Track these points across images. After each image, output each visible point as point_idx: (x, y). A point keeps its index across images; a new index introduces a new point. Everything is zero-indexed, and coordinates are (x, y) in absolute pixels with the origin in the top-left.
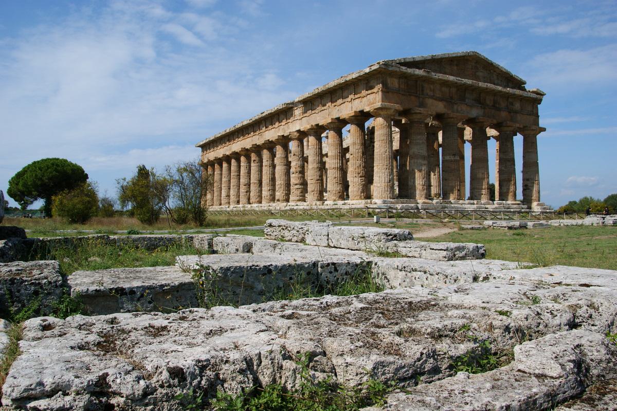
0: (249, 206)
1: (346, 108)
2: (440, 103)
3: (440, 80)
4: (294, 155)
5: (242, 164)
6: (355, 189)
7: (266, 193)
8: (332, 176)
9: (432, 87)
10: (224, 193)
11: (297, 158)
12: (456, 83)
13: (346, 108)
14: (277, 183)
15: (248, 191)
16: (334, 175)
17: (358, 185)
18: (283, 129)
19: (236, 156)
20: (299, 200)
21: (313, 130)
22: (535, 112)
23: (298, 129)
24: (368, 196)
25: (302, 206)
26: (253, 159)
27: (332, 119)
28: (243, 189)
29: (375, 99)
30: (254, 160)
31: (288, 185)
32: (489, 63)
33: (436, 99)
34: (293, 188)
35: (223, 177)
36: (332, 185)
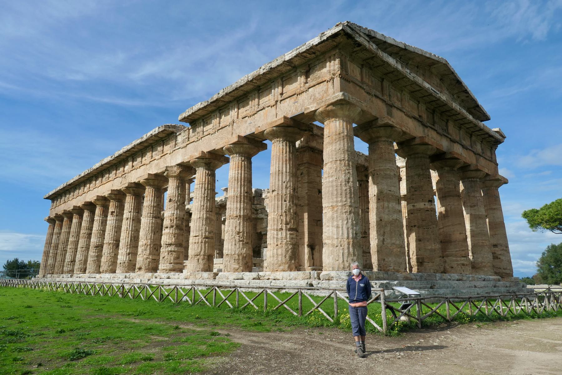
0: (98, 276)
3: (415, 83)
4: (170, 200)
5: (96, 218)
6: (280, 251)
7: (122, 256)
8: (231, 229)
9: (399, 94)
10: (68, 258)
11: (173, 205)
12: (431, 95)
15: (99, 257)
16: (237, 229)
17: (286, 244)
18: (157, 165)
19: (90, 206)
20: (171, 270)
23: (179, 161)
26: (111, 209)
27: (239, 136)
28: (92, 253)
29: (326, 91)
31: (156, 247)
33: (407, 115)
34: (164, 251)
35: (71, 236)
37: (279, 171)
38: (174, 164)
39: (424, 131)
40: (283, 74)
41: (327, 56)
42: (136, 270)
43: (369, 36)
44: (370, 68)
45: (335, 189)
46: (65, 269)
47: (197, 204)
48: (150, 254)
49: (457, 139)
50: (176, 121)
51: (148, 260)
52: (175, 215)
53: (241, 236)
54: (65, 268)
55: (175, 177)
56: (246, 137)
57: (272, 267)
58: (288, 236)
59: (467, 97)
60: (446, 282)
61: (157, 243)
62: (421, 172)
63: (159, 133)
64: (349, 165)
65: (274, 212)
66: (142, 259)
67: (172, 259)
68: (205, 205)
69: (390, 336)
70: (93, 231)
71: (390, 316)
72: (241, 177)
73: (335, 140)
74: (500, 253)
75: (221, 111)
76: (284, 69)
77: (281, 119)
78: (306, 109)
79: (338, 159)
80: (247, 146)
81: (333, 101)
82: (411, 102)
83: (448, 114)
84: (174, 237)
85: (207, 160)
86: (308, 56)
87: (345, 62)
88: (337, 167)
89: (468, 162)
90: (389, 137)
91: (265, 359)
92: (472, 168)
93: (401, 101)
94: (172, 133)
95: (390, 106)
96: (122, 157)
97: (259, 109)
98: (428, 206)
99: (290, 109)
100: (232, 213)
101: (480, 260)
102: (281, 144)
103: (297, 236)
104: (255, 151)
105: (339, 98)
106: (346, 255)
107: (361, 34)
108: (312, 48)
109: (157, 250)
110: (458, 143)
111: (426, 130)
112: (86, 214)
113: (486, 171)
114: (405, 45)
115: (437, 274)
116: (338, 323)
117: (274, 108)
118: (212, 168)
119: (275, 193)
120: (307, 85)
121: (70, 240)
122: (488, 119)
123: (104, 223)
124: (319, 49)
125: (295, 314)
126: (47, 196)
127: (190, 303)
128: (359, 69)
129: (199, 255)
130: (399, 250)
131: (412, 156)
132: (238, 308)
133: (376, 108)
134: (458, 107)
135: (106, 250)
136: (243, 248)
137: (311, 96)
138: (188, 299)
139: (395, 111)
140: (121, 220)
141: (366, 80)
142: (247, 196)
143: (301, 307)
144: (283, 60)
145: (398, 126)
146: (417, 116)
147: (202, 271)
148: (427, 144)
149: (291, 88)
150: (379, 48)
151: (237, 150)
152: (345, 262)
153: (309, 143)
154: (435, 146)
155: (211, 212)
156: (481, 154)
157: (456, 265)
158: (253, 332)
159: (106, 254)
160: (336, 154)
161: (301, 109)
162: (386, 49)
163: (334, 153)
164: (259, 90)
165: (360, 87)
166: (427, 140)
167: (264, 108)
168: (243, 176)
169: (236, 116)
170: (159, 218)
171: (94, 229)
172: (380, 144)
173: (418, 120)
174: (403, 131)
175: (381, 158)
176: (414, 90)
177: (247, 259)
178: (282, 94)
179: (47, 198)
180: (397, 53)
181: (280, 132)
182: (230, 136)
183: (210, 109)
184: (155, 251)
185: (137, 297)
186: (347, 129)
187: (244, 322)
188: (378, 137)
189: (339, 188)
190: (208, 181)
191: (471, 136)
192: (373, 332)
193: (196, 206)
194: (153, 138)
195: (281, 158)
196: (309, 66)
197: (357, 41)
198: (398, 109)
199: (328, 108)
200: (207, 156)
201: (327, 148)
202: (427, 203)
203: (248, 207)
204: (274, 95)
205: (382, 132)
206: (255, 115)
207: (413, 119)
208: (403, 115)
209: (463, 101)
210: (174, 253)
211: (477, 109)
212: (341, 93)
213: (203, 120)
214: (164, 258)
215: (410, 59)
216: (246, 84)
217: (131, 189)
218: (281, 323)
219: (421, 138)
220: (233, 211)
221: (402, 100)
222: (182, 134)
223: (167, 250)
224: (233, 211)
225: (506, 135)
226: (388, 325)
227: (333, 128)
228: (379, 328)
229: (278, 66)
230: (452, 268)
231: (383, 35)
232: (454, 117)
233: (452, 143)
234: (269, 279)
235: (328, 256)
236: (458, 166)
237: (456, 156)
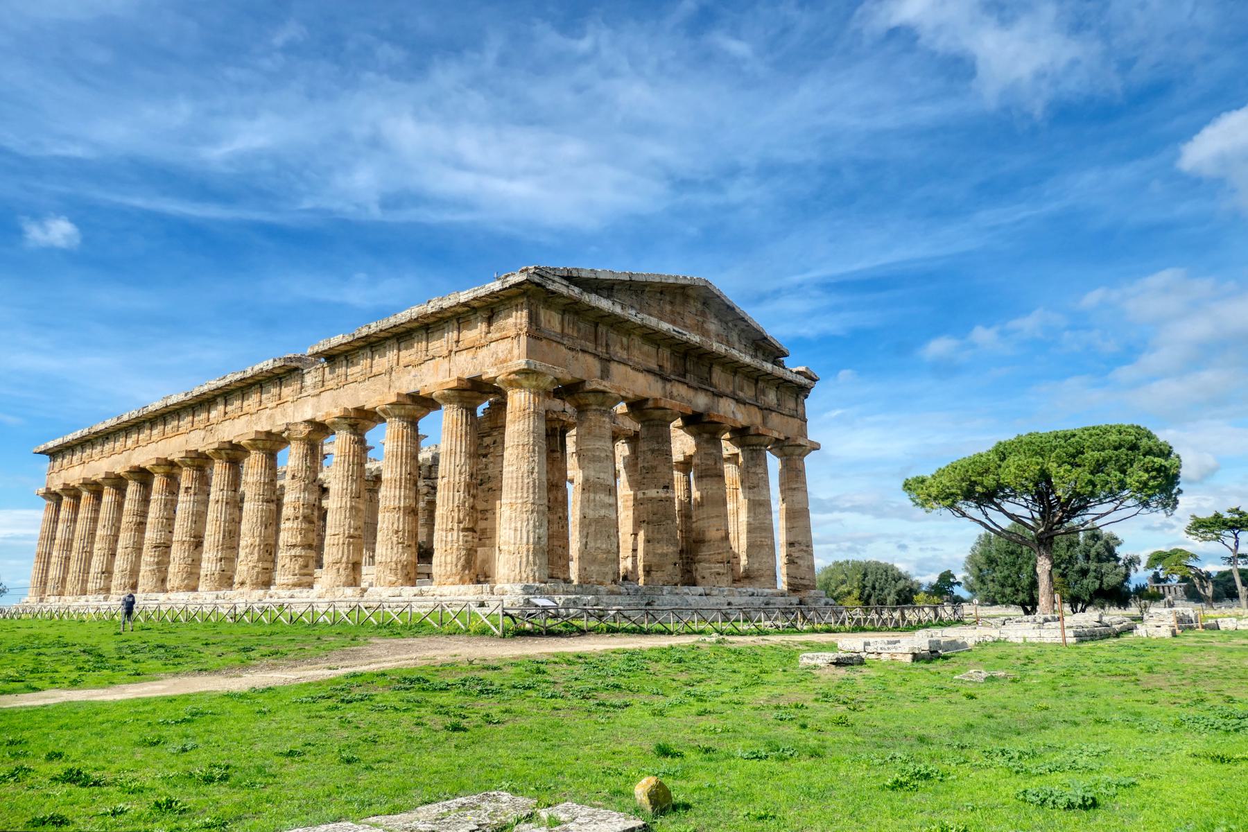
0: (162, 597)
1: (435, 368)
2: (640, 375)
3: (643, 326)
4: (294, 477)
5: (154, 496)
7: (209, 562)
9: (625, 340)
11: (298, 483)
12: (673, 337)
13: (435, 368)
14: (242, 543)
17: (458, 549)
18: (271, 417)
21: (348, 421)
22: (800, 411)
23: (308, 417)
27: (399, 395)
28: (148, 557)
29: (511, 351)
30: (187, 488)
31: (269, 550)
32: (728, 307)
34: (283, 556)
35: (100, 526)
36: (388, 548)
39: (664, 388)
46: (90, 586)
48: (258, 561)
49: (728, 391)
54: (89, 585)
55: (300, 440)
56: (408, 395)
62: (656, 446)
64: (534, 451)
82: (646, 348)
92: (752, 431)
93: (627, 348)
94: (296, 369)
95: (606, 361)
99: (466, 366)
101: (756, 566)
111: (668, 386)
113: (776, 435)
119: (445, 480)
121: (98, 533)
123: (170, 506)
126: (42, 448)
133: (584, 367)
135: (177, 552)
136: (403, 553)
140: (206, 503)
141: (568, 331)
166: (662, 404)
167: (434, 358)
178: (458, 342)
182: (386, 390)
183: (357, 344)
184: (267, 555)
185: (257, 622)
191: (757, 381)
193: (334, 474)
198: (619, 362)
208: (629, 369)
219: (656, 400)
227: (518, 400)
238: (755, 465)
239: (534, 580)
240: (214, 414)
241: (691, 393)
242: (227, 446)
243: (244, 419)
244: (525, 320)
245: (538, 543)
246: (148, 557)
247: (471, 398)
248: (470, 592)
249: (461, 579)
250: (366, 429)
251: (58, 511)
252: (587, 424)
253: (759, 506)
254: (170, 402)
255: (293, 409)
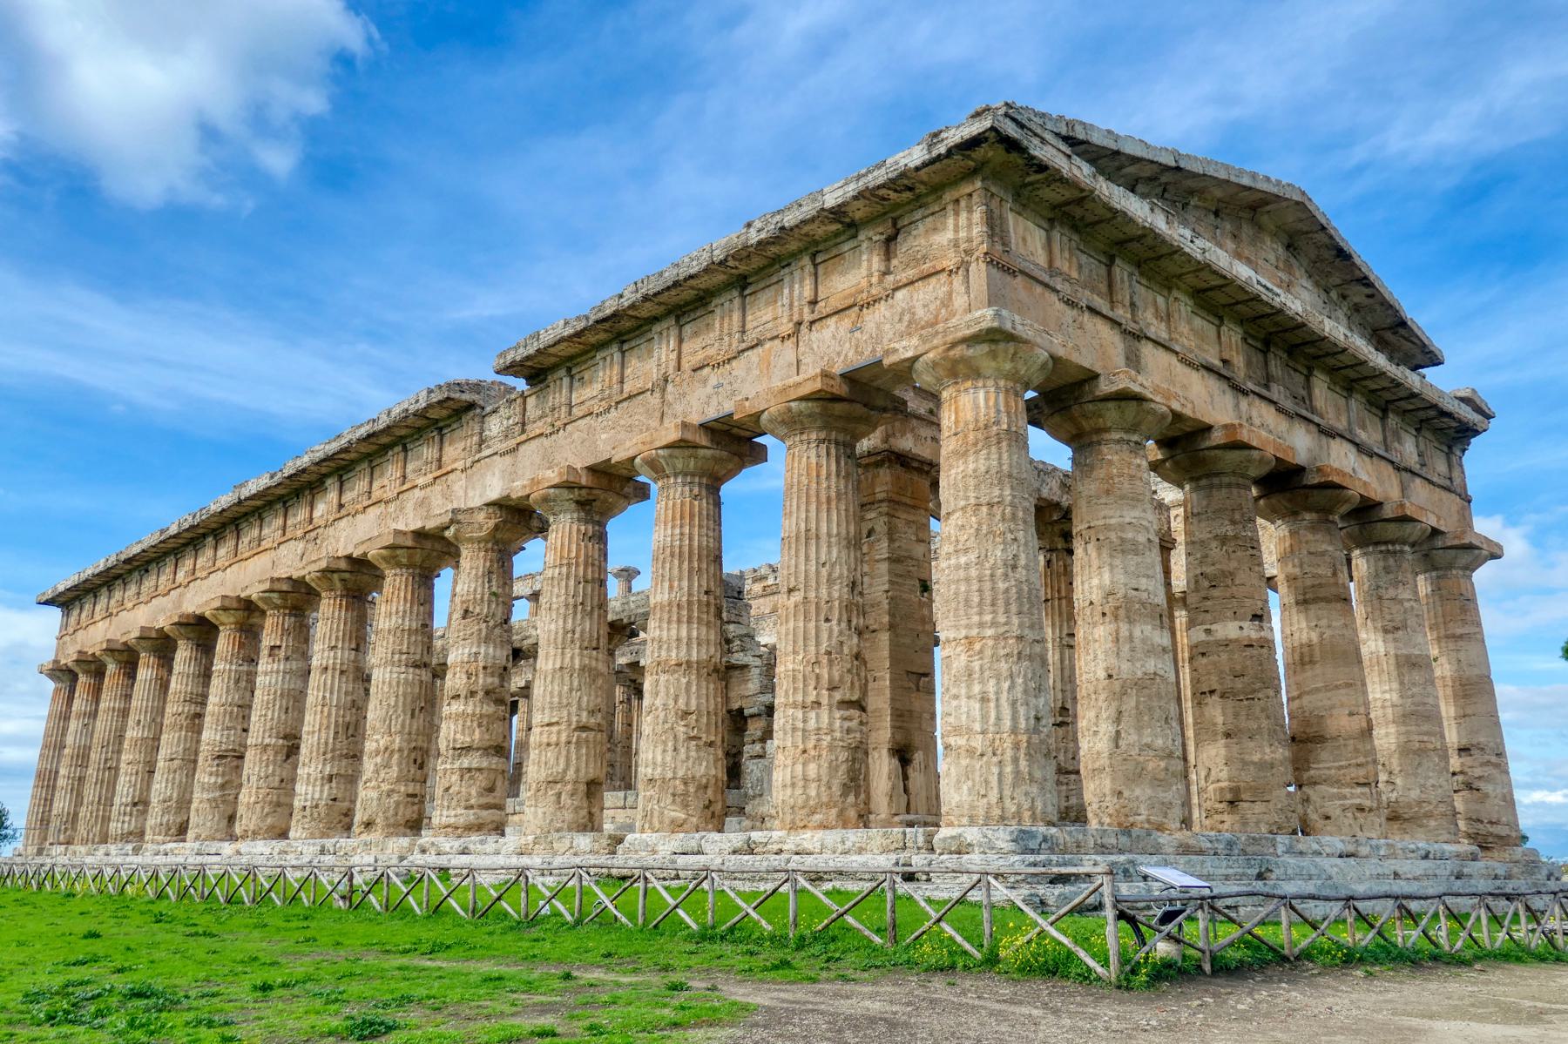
0: (228, 848)
1: (769, 360)
3: (1206, 267)
5: (218, 666)
6: (812, 769)
7: (309, 788)
9: (1160, 300)
10: (124, 791)
12: (1256, 298)
13: (769, 360)
14: (369, 746)
17: (831, 748)
18: (423, 503)
22: (1457, 481)
23: (494, 495)
24: (919, 807)
25: (492, 859)
26: (267, 640)
28: (206, 776)
29: (947, 301)
30: (272, 648)
31: (419, 758)
34: (445, 771)
37: (807, 530)
38: (476, 502)
39: (1237, 406)
40: (816, 243)
41: (948, 196)
42: (356, 829)
43: (1069, 140)
44: (1075, 228)
45: (975, 587)
47: (553, 627)
48: (398, 780)
49: (1341, 425)
50: (483, 371)
51: (395, 797)
52: (481, 657)
53: (693, 723)
54: (112, 825)
56: (704, 427)
57: (788, 818)
58: (838, 723)
59: (1369, 296)
60: (1305, 862)
61: (420, 743)
62: (1229, 530)
63: (430, 406)
65: (795, 652)
66: (375, 795)
67: (474, 792)
68: (578, 629)
69: (1128, 989)
70: (210, 708)
71: (1131, 940)
72: (690, 546)
73: (975, 444)
74: (1478, 772)
75: (625, 347)
76: (820, 231)
77: (814, 378)
78: (887, 352)
79: (984, 500)
80: (708, 453)
81: (968, 332)
82: (1198, 322)
83: (1311, 350)
84: (480, 725)
85: (584, 492)
86: (893, 195)
87: (1001, 217)
88: (980, 524)
89: (1372, 495)
90: (1133, 428)
91: (829, 1030)
92: (1388, 512)
93: (1168, 318)
94: (471, 406)
95: (1136, 337)
96: (305, 478)
97: (744, 346)
98: (1251, 631)
99: (835, 349)
100: (664, 653)
102: (813, 453)
103: (861, 723)
104: (730, 466)
105: (985, 325)
106: (1009, 779)
107: (1048, 136)
108: (903, 175)
109: (421, 767)
110: (1342, 437)
111: (1244, 403)
112: (183, 655)
113: (1432, 521)
114: (1176, 154)
115: (1279, 838)
116: (992, 960)
117: (789, 343)
118: (597, 518)
119: (797, 597)
120: (890, 278)
121: (129, 734)
122: (1435, 360)
123: (246, 682)
124: (925, 178)
125: (877, 940)
126: (49, 595)
127: (569, 918)
128: (1043, 233)
129: (561, 781)
130: (1163, 764)
131: (1203, 482)
132: (713, 927)
133: (1093, 347)
134: (1342, 330)
135: (252, 766)
137: (902, 314)
138: (561, 908)
139: (1147, 350)
141: (1062, 263)
142: (708, 604)
143: (894, 920)
144: (818, 205)
145: (1158, 399)
146: (1217, 363)
147: (570, 830)
148: (1246, 447)
149: (841, 287)
150: (1101, 171)
151: (679, 465)
152: (1008, 802)
153: (892, 440)
154: (1270, 451)
155: (596, 649)
156: (1416, 468)
157: (1338, 812)
158: (774, 982)
159: (254, 779)
160: (977, 487)
161: (874, 350)
162: (1119, 168)
163: (972, 482)
164: (744, 288)
165: (1047, 286)
166: (1244, 436)
167: (759, 344)
168: (696, 543)
169: (673, 364)
170: (425, 665)
171: (213, 699)
172: (1104, 449)
173: (1220, 373)
174: (1172, 411)
175: (1108, 492)
176: (1205, 285)
177: (710, 792)
179: (47, 603)
180: (1152, 179)
181: (809, 416)
182: (654, 423)
183: (592, 339)
185: (396, 909)
186: (1008, 413)
187: (742, 962)
188: (1099, 431)
189: (987, 585)
190: (587, 556)
191: (1385, 411)
192: (1086, 978)
194: (409, 422)
195: (813, 492)
196: (895, 224)
197: (1033, 157)
198: (1157, 343)
199: (951, 353)
200: (584, 481)
201: (951, 466)
202: (1246, 624)
203: (712, 637)
204: (791, 305)
205: (1111, 413)
206: (734, 363)
207: (1203, 372)
208: (1174, 360)
209: (1357, 308)
210: (480, 776)
211: (1402, 331)
212: (989, 312)
213: (569, 370)
214: (447, 790)
215: (1191, 192)
216: (706, 270)
217: (336, 576)
218: (841, 964)
220: (669, 650)
221: (1168, 315)
222: (502, 411)
223: (457, 765)
224: (669, 650)
225: (1492, 405)
226: (1124, 960)
227: (969, 407)
228: (1099, 970)
229: (804, 222)
230: (1328, 818)
231: (1109, 132)
232: (1331, 361)
233: (1324, 439)
234: (781, 851)
235: (957, 781)
236: (1345, 509)
237: (1336, 479)
238: (1396, 583)
239: (1034, 817)
240: (321, 509)
241: (1282, 424)
242: (343, 565)
243: (374, 512)
244: (978, 230)
245: (1036, 731)
246: (206, 776)
247: (848, 418)
248: (869, 852)
249: (841, 813)
250: (607, 512)
251: (71, 699)
252: (1100, 473)
253: (1411, 665)
254: (245, 493)
255: (465, 484)
